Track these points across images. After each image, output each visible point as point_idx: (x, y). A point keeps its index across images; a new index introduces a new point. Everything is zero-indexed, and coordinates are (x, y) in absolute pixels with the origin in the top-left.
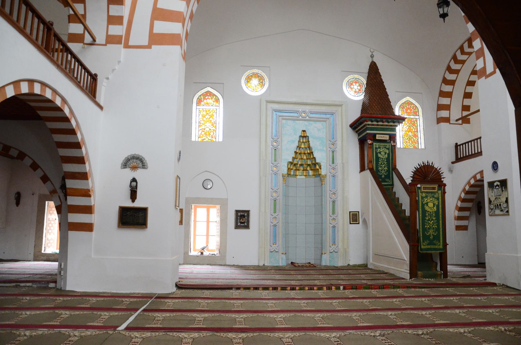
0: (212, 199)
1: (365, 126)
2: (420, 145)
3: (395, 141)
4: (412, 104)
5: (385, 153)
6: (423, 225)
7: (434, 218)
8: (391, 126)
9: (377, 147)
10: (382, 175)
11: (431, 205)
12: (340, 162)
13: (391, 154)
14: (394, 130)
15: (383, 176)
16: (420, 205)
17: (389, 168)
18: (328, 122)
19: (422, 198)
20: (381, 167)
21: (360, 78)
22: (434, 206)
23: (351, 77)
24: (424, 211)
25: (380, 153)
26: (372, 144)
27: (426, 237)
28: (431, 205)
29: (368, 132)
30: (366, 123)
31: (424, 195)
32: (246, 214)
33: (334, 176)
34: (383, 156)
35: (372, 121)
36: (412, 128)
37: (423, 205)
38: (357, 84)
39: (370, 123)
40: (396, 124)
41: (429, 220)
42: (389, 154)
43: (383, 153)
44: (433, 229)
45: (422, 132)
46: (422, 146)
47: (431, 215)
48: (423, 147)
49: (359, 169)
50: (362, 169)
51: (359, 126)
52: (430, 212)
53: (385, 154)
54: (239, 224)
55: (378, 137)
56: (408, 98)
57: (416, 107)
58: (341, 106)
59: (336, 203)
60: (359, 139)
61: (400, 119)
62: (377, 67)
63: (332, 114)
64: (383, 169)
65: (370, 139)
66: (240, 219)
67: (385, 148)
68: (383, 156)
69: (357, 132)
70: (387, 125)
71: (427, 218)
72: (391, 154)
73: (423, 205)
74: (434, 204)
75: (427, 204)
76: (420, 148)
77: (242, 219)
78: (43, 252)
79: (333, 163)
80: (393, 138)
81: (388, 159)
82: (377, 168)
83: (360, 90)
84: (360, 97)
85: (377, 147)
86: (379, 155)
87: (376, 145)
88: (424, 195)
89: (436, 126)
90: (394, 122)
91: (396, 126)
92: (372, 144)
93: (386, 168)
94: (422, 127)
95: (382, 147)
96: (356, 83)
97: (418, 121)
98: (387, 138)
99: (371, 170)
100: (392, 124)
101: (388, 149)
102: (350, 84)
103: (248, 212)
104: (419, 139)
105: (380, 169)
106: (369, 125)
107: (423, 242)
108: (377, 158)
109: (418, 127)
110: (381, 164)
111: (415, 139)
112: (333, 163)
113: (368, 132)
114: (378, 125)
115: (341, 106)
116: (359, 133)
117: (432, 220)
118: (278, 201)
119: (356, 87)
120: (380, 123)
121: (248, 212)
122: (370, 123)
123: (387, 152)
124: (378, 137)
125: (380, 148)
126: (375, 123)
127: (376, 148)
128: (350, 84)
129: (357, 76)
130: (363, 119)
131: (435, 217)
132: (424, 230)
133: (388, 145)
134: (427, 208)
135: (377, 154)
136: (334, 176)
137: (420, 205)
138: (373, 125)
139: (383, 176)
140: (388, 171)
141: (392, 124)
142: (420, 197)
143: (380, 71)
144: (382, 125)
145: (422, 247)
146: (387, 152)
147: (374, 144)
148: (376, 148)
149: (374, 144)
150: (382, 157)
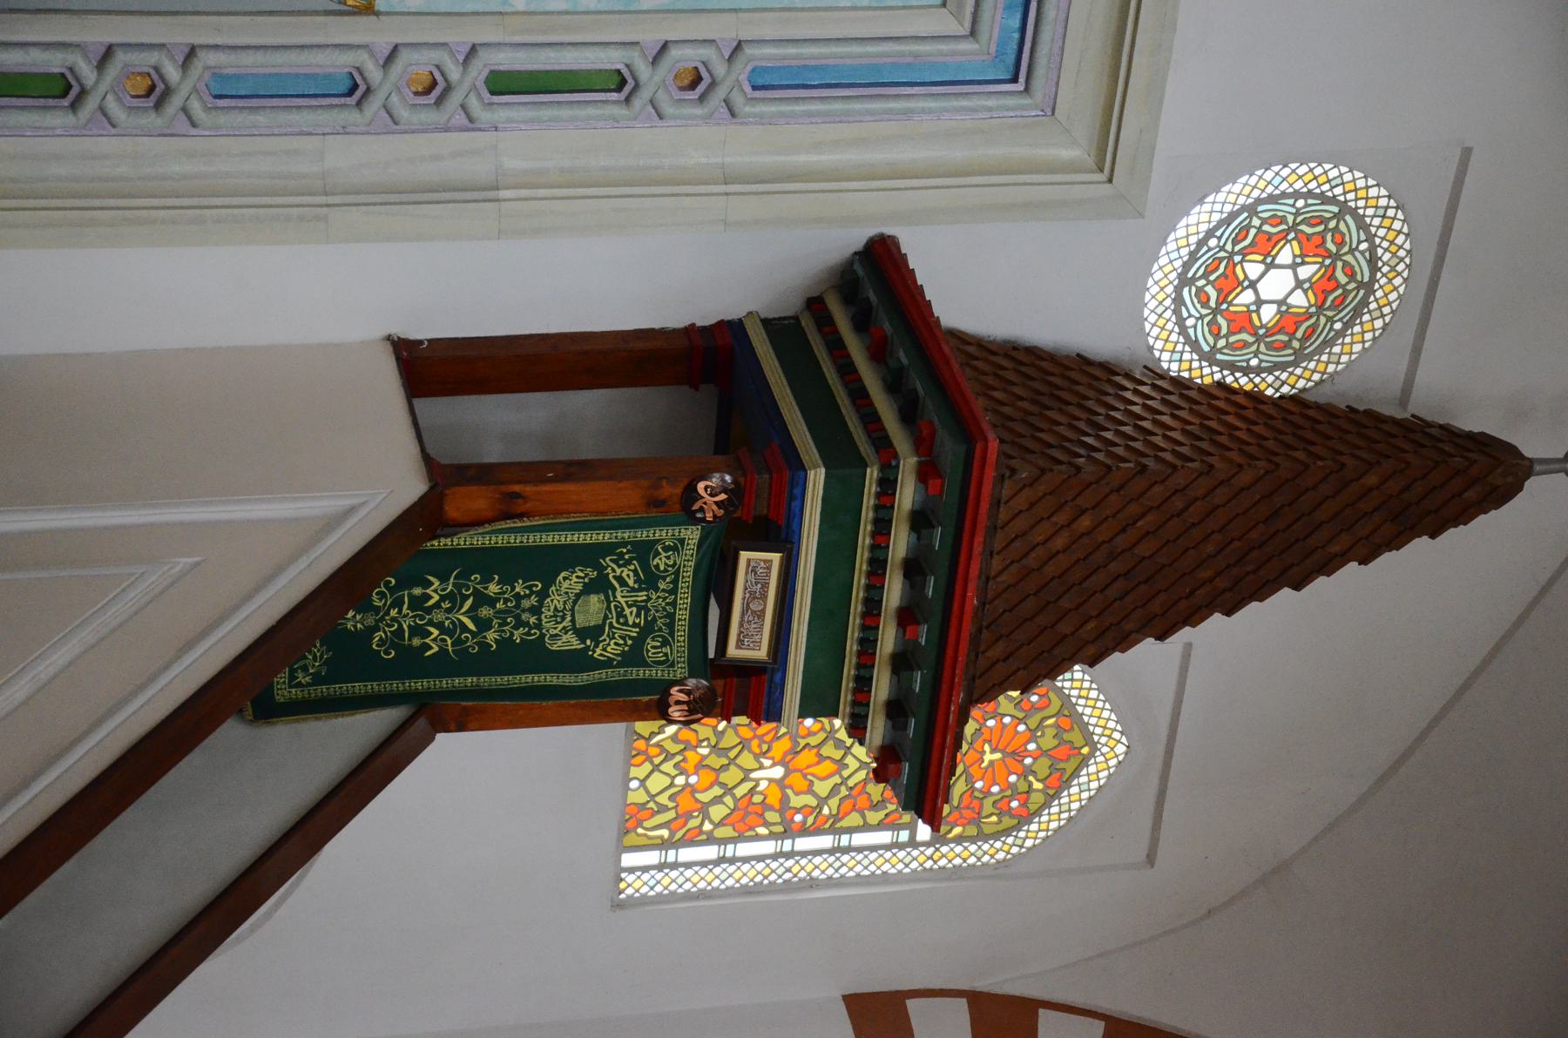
1: (883, 444)
2: (652, 857)
3: (700, 708)
4: (1058, 784)
5: (594, 633)
8: (863, 683)
9: (660, 561)
10: (365, 606)
12: (511, 164)
13: (584, 678)
14: (818, 703)
15: (353, 620)
17: (442, 665)
18: (951, 26)
20: (454, 599)
21: (1370, 326)
23: (1394, 236)
25: (599, 585)
26: (687, 509)
29: (817, 479)
30: (908, 464)
33: (354, 90)
34: (566, 611)
35: (920, 520)
36: (822, 788)
38: (1299, 300)
39: (907, 495)
40: (877, 728)
45: (778, 872)
46: (643, 871)
48: (633, 886)
49: (424, 329)
50: (430, 369)
51: (878, 354)
53: (582, 634)
55: (756, 566)
56: (1112, 749)
57: (1025, 817)
58: (1104, 156)
59: (59, 119)
60: (729, 333)
61: (919, 775)
62: (1463, 516)
63: (1019, 69)
64: (439, 617)
65: (736, 494)
67: (647, 630)
68: (566, 611)
69: (815, 304)
70: (868, 646)
72: (584, 678)
76: (628, 860)
79: (503, 85)
80: (743, 691)
81: (536, 655)
82: (445, 563)
83: (1243, 321)
84: (1171, 344)
85: (660, 561)
86: (570, 581)
89: (831, 993)
90: (896, 710)
91: (857, 729)
92: (691, 518)
93: (434, 641)
94: (822, 868)
95: (657, 600)
96: (1322, 288)
97: (885, 837)
99: (423, 518)
100: (882, 687)
101: (634, 656)
102: (1321, 231)
104: (710, 852)
105: (435, 590)
106: (888, 486)
108: (543, 566)
109: (826, 841)
110: (482, 599)
111: (718, 812)
112: (503, 85)
113: (817, 479)
114: (878, 567)
115: (1104, 156)
116: (799, 331)
119: (1277, 285)
120: (894, 592)
122: (907, 495)
124: (756, 566)
125: (649, 580)
126: (900, 543)
127: (644, 551)
128: (1321, 231)
129: (1390, 291)
130: (949, 449)
133: (669, 657)
135: (589, 556)
136: (354, 90)
138: (882, 527)
139: (353, 620)
140: (411, 661)
141: (882, 687)
143: (1421, 544)
144: (873, 606)
146: (610, 648)
147: (692, 534)
148: (644, 551)
149: (692, 534)
150: (555, 601)
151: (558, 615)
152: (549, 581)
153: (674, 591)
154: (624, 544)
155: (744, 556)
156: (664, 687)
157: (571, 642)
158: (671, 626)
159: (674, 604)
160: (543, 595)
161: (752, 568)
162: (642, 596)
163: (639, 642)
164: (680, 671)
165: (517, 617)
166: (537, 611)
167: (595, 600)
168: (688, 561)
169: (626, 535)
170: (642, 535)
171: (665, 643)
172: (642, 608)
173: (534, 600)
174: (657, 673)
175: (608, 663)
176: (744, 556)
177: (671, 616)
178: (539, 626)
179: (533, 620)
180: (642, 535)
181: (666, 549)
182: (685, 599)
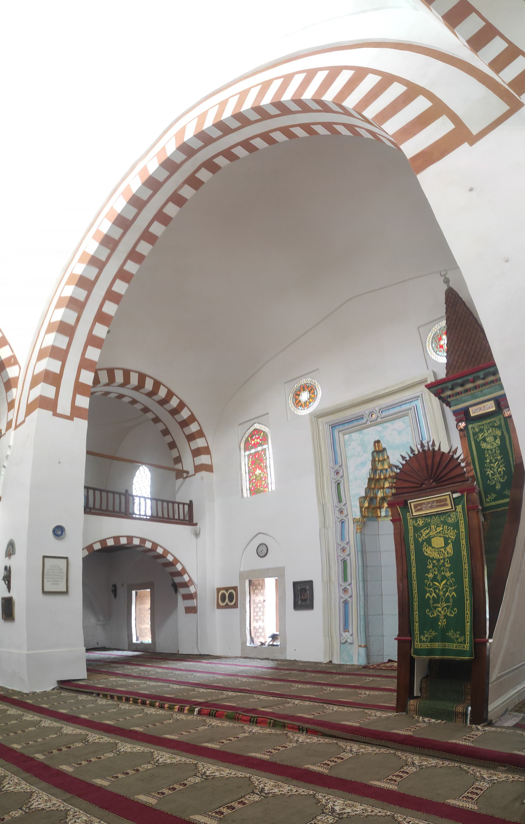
0: (268, 569)
5: (495, 438)
6: (422, 592)
7: (448, 574)
11: (438, 542)
16: (412, 547)
19: (417, 529)
22: (446, 544)
24: (423, 560)
25: (484, 440)
27: (429, 623)
28: (438, 542)
31: (421, 522)
32: (307, 587)
37: (419, 547)
41: (435, 579)
42: (502, 438)
43: (490, 439)
44: (447, 600)
47: (440, 567)
52: (438, 560)
54: (300, 602)
55: (474, 412)
66: (301, 595)
67: (493, 427)
68: (491, 443)
71: (431, 576)
73: (419, 547)
74: (446, 540)
75: (428, 541)
77: (303, 595)
78: (134, 641)
85: (477, 430)
86: (484, 445)
87: (473, 428)
88: (421, 522)
98: (491, 407)
101: (499, 427)
103: (310, 583)
107: (421, 633)
108: (481, 452)
117: (444, 577)
118: (348, 562)
121: (310, 583)
123: (498, 433)
124: (474, 412)
125: (481, 431)
127: (475, 434)
131: (450, 569)
132: (424, 604)
134: (428, 551)
135: (478, 444)
137: (412, 547)
142: (411, 528)
145: (418, 645)
146: (498, 433)
147: (470, 426)
149: (470, 426)
150: (489, 447)
151: (492, 445)
152: (485, 450)
153: (483, 425)
154: (474, 438)
155: (472, 415)
156: (506, 419)
157: (498, 441)
158: (491, 422)
159: (486, 424)
160: (488, 450)
161: (475, 412)
162: (485, 431)
163: (495, 427)
164: (501, 416)
165: (494, 454)
166: (492, 450)
167: (487, 439)
168: (476, 425)
169: (472, 439)
170: (471, 435)
171: (495, 422)
172: (488, 429)
173: (490, 452)
174: (502, 421)
175: (502, 432)
176: (472, 415)
177: (489, 423)
178: (495, 448)
179: (494, 450)
180: (471, 435)
181: (474, 430)
182: (485, 422)
